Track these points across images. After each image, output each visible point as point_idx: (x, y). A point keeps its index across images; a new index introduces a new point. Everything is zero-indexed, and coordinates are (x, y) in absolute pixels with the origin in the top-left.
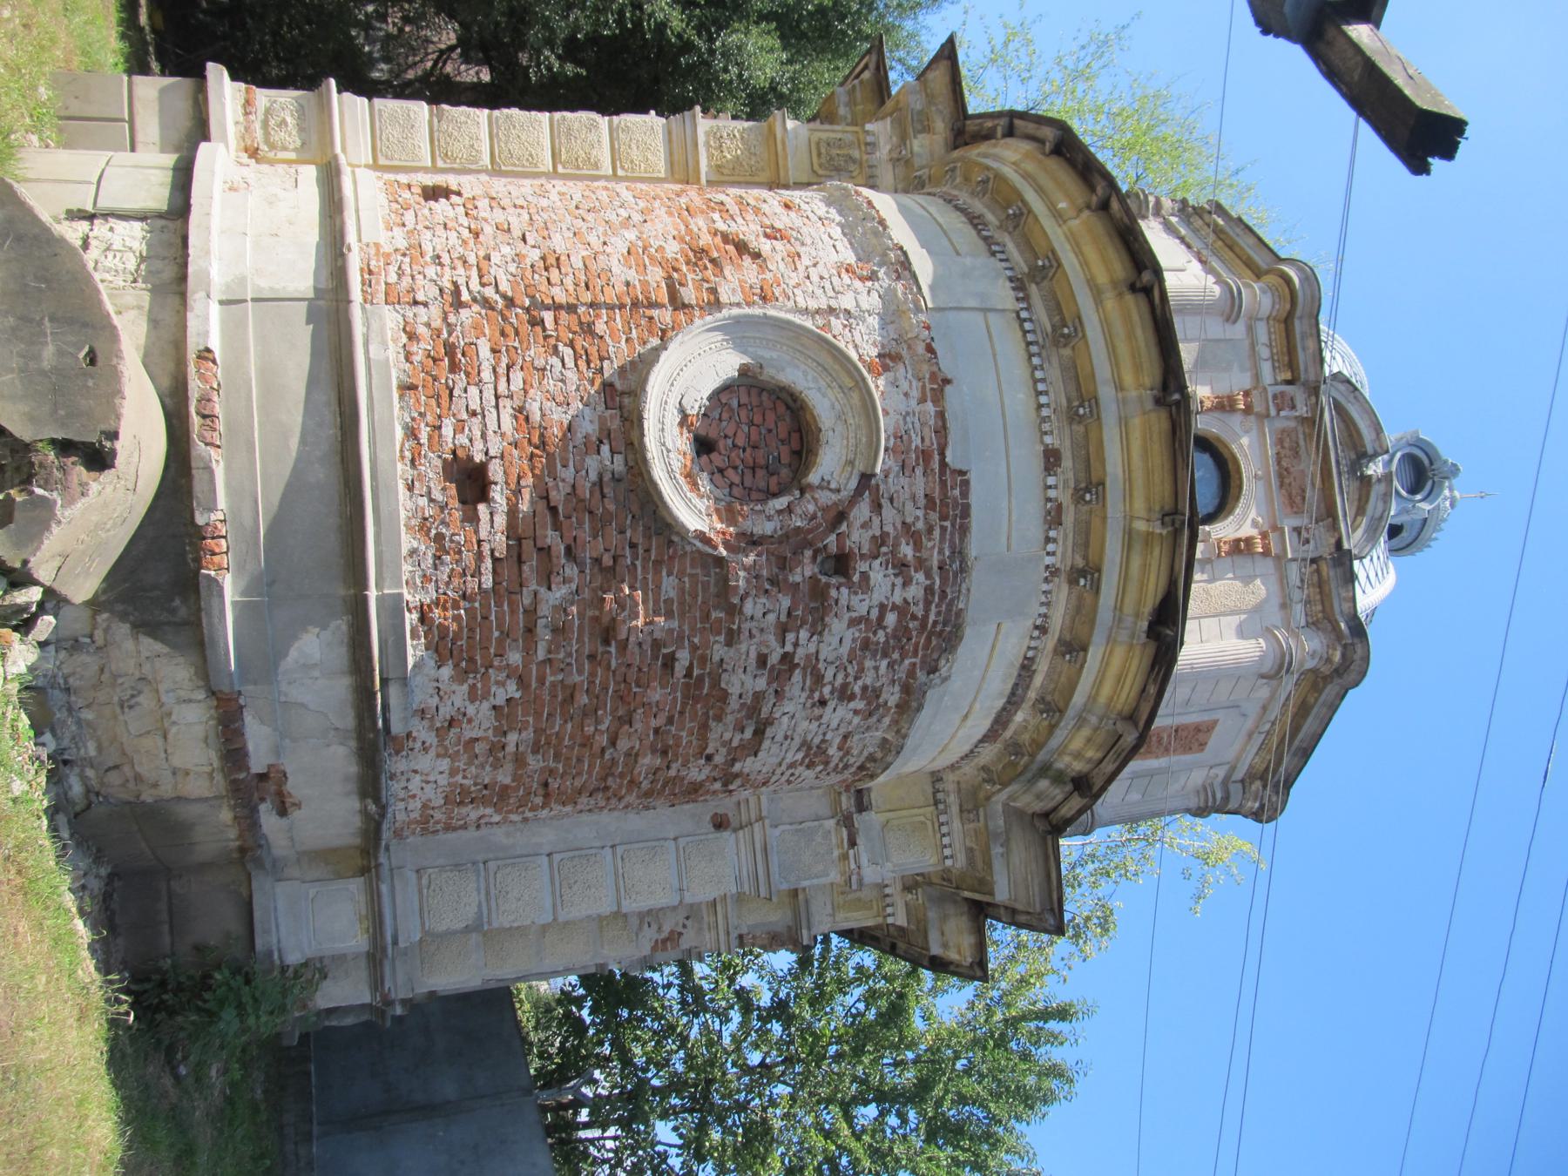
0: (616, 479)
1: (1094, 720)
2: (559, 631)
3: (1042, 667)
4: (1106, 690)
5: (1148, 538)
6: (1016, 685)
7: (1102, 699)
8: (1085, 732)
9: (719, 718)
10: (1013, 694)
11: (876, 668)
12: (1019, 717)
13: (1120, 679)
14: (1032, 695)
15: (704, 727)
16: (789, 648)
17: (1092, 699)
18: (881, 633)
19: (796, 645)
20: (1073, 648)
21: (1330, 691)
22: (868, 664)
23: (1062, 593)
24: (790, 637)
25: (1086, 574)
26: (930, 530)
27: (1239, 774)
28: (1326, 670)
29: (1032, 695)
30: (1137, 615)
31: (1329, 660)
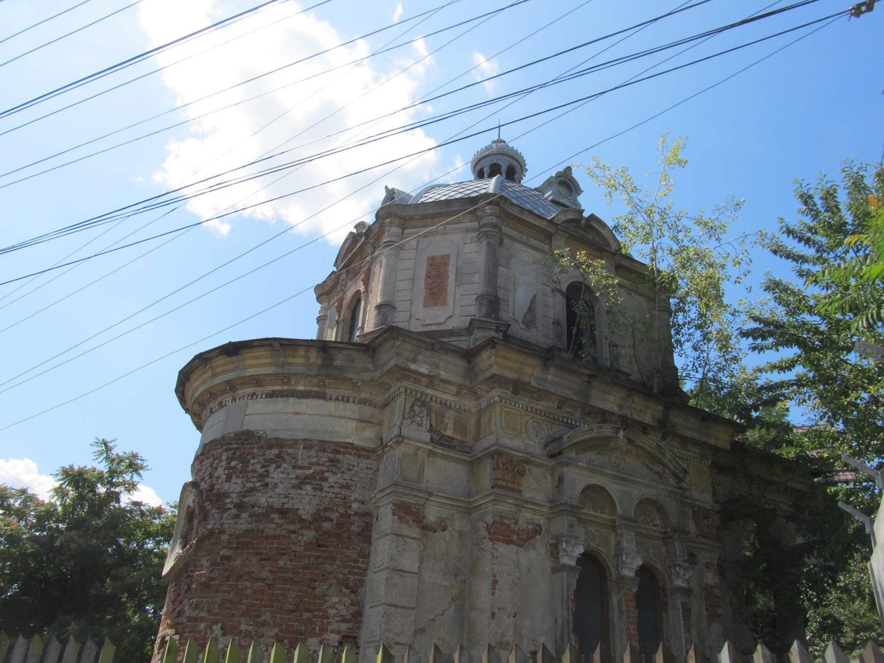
0: (176, 585)
1: (281, 359)
2: (197, 607)
3: (270, 389)
4: (263, 361)
5: (212, 368)
6: (282, 396)
7: (269, 360)
8: (290, 360)
9: (262, 532)
10: (287, 396)
11: (253, 464)
12: (301, 388)
13: (257, 358)
14: (286, 388)
15: (267, 537)
16: (232, 506)
17: (271, 364)
18: (239, 466)
19: (232, 503)
20: (258, 381)
21: (407, 213)
22: (250, 468)
23: (241, 392)
24: (229, 506)
25: (231, 386)
26: (212, 455)
27: (475, 224)
28: (397, 221)
29: (286, 388)
30: (233, 362)
31: (391, 223)
